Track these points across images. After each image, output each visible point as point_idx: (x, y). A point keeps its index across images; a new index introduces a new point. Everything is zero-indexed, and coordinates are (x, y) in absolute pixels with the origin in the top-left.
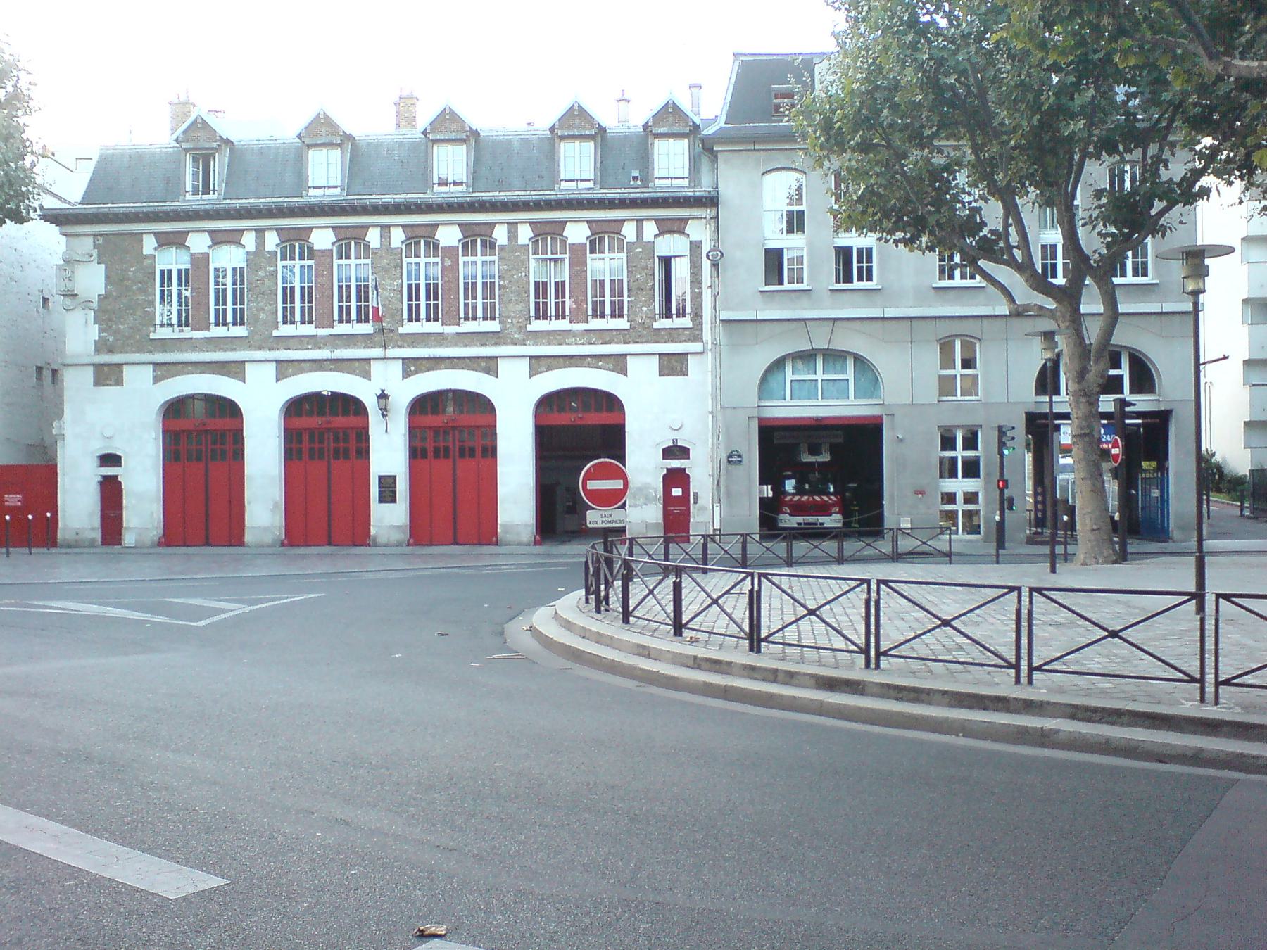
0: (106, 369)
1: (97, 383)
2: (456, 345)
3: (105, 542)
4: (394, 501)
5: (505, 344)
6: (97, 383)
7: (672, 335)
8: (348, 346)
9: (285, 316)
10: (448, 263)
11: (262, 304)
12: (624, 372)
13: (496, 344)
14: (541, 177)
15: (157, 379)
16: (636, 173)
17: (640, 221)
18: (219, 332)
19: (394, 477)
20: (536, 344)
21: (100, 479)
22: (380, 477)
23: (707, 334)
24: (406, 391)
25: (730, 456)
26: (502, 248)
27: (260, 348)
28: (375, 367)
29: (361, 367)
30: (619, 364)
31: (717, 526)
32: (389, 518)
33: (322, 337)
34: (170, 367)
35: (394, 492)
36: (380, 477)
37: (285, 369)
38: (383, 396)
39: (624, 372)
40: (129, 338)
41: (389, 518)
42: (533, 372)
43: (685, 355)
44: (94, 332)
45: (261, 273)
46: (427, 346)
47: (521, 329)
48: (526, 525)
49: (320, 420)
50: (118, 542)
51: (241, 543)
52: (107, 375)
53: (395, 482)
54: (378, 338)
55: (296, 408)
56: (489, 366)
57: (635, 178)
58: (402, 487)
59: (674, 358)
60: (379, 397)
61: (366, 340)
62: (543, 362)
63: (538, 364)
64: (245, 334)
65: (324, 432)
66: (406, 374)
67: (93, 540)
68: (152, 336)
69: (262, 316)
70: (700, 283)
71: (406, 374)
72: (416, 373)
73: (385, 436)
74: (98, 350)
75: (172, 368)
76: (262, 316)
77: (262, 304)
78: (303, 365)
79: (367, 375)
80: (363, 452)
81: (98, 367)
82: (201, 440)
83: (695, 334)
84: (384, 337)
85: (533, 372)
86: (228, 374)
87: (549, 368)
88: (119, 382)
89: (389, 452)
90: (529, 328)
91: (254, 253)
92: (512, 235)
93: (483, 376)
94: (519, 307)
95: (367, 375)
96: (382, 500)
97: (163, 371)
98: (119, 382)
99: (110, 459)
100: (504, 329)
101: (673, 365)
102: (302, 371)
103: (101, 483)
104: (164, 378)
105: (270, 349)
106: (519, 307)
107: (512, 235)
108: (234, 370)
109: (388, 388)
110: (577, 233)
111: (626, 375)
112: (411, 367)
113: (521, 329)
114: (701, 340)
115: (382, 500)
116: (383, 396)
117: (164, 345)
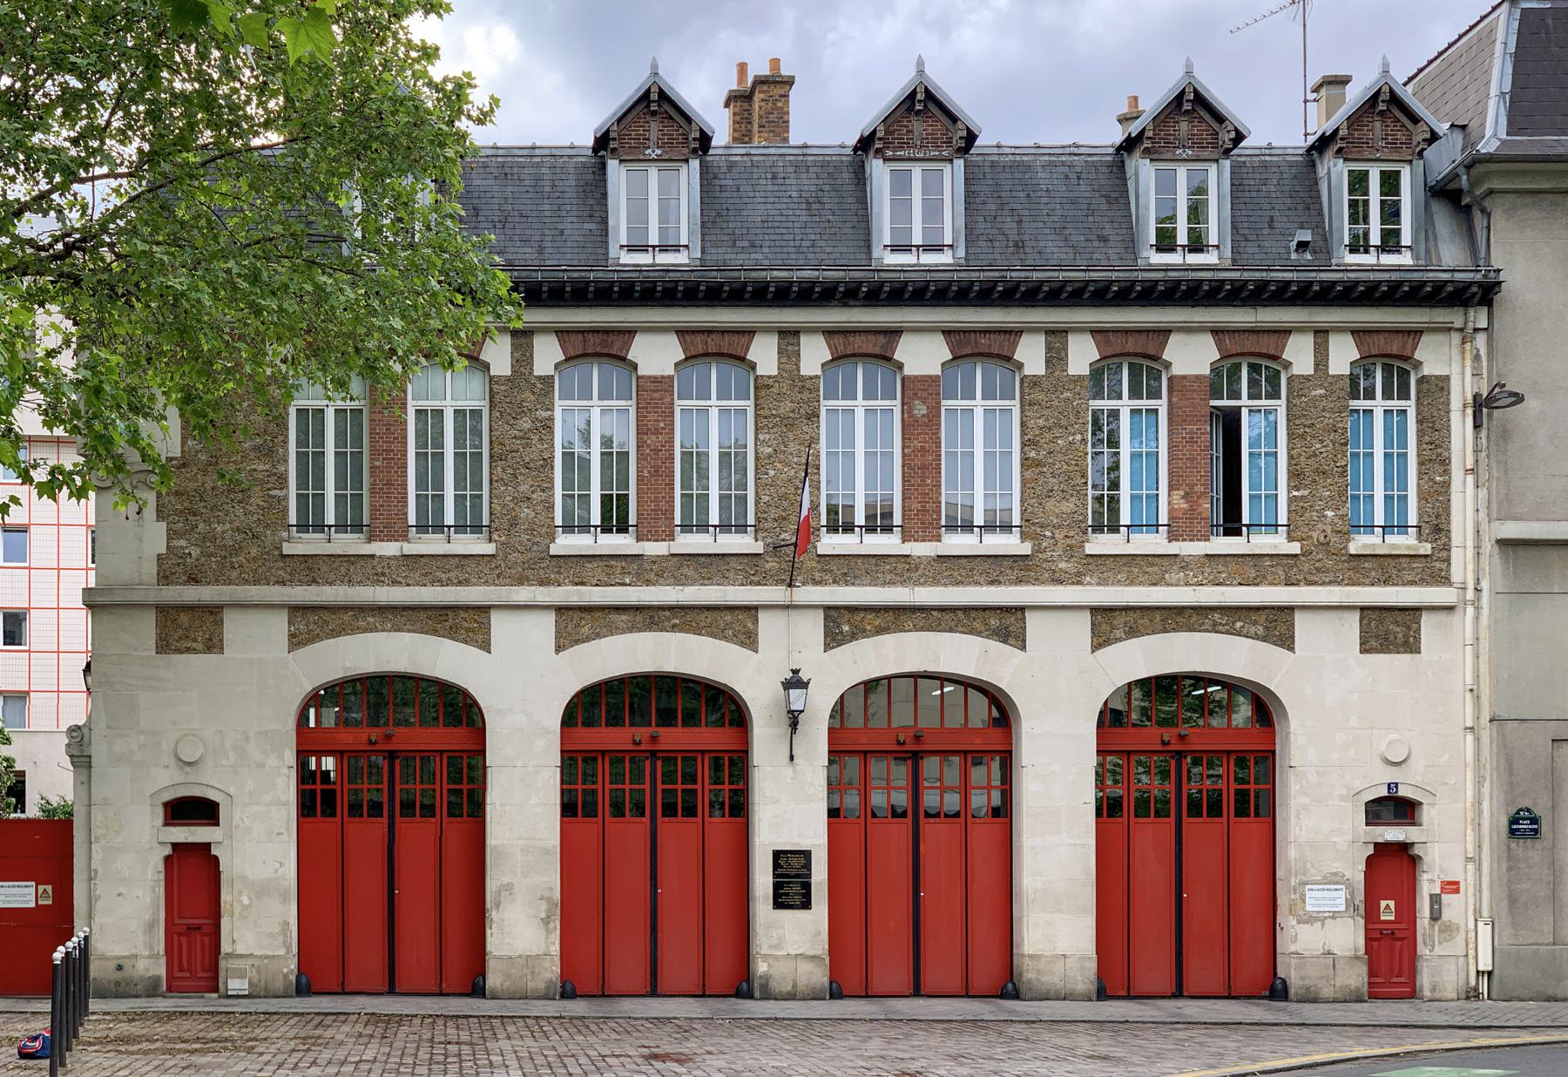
0: (184, 618)
1: (165, 645)
2: (935, 582)
3: (175, 986)
4: (806, 905)
5: (1038, 581)
6: (165, 645)
7: (1386, 567)
8: (707, 580)
9: (568, 514)
10: (920, 409)
11: (523, 488)
12: (1286, 641)
13: (1019, 581)
14: (1104, 239)
15: (297, 641)
16: (1306, 236)
17: (1321, 334)
18: (431, 545)
19: (807, 855)
20: (1103, 582)
21: (168, 851)
22: (777, 855)
23: (1461, 564)
24: (838, 672)
25: (1514, 821)
26: (1035, 382)
27: (521, 581)
28: (768, 625)
29: (737, 624)
30: (1275, 625)
31: (1485, 964)
32: (791, 941)
33: (655, 560)
34: (326, 616)
35: (807, 886)
36: (777, 855)
37: (576, 624)
38: (795, 682)
39: (1286, 641)
40: (236, 550)
41: (791, 941)
42: (1100, 641)
43: (1416, 610)
44: (156, 537)
45: (525, 423)
46: (874, 582)
47: (1071, 551)
48: (1083, 958)
49: (641, 733)
50: (212, 983)
51: (477, 990)
52: (188, 629)
53: (808, 866)
54: (772, 564)
55: (593, 706)
56: (1007, 625)
57: (1302, 246)
58: (819, 874)
59: (1388, 616)
60: (788, 685)
61: (748, 567)
62: (1119, 620)
63: (1110, 624)
64: (489, 549)
65: (657, 756)
66: (833, 639)
67: (155, 981)
68: (288, 549)
69: (526, 512)
70: (1445, 463)
71: (833, 639)
72: (853, 637)
73: (788, 772)
74: (165, 578)
75: (333, 621)
76: (526, 512)
77: (523, 488)
78: (614, 617)
79: (749, 640)
80: (739, 807)
81: (165, 612)
82: (391, 769)
83: (1434, 569)
84: (791, 556)
85: (1100, 641)
86: (452, 634)
87: (1132, 633)
88: (214, 645)
89: (790, 805)
90: (1090, 549)
91: (509, 379)
92: (1056, 357)
93: (995, 646)
94: (1068, 506)
95: (749, 640)
96: (780, 902)
97: (311, 624)
98: (214, 645)
99: (194, 809)
100: (1038, 550)
101: (1390, 631)
102: (613, 630)
103: (168, 860)
104: (312, 639)
105: (543, 583)
106: (1068, 506)
107: (1056, 357)
108: (468, 624)
109: (787, 671)
110: (1191, 356)
111: (1291, 649)
112: (843, 625)
113: (1071, 551)
114: (1446, 580)
115: (780, 902)
116: (795, 682)
117: (310, 568)
